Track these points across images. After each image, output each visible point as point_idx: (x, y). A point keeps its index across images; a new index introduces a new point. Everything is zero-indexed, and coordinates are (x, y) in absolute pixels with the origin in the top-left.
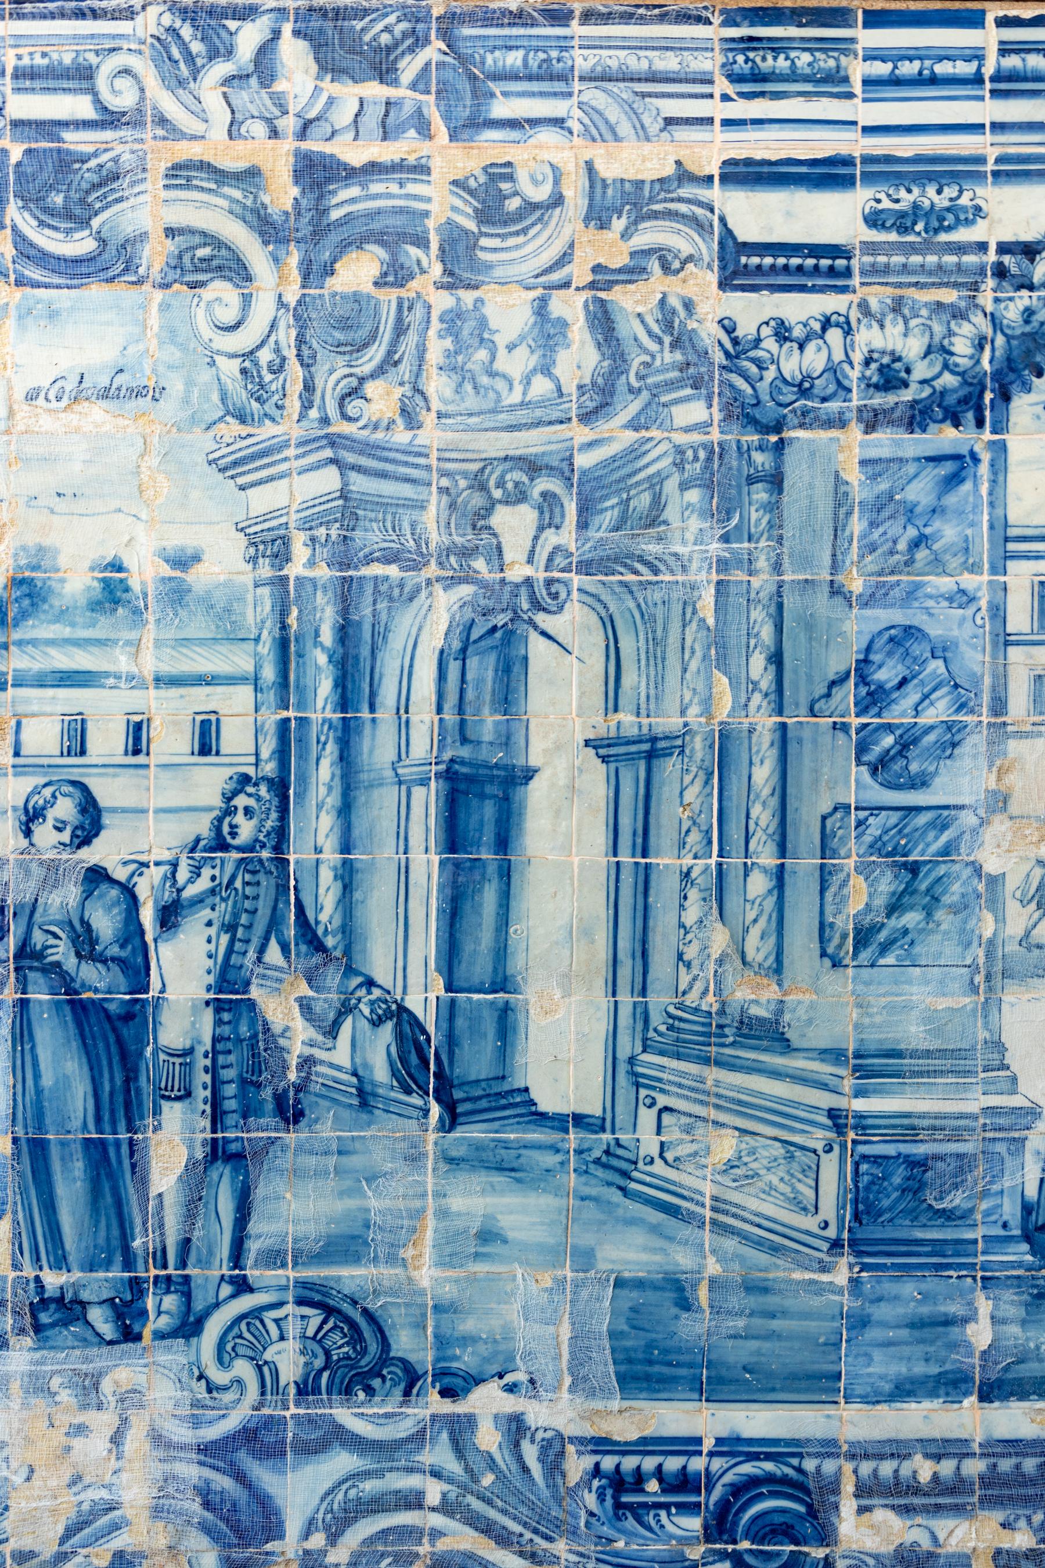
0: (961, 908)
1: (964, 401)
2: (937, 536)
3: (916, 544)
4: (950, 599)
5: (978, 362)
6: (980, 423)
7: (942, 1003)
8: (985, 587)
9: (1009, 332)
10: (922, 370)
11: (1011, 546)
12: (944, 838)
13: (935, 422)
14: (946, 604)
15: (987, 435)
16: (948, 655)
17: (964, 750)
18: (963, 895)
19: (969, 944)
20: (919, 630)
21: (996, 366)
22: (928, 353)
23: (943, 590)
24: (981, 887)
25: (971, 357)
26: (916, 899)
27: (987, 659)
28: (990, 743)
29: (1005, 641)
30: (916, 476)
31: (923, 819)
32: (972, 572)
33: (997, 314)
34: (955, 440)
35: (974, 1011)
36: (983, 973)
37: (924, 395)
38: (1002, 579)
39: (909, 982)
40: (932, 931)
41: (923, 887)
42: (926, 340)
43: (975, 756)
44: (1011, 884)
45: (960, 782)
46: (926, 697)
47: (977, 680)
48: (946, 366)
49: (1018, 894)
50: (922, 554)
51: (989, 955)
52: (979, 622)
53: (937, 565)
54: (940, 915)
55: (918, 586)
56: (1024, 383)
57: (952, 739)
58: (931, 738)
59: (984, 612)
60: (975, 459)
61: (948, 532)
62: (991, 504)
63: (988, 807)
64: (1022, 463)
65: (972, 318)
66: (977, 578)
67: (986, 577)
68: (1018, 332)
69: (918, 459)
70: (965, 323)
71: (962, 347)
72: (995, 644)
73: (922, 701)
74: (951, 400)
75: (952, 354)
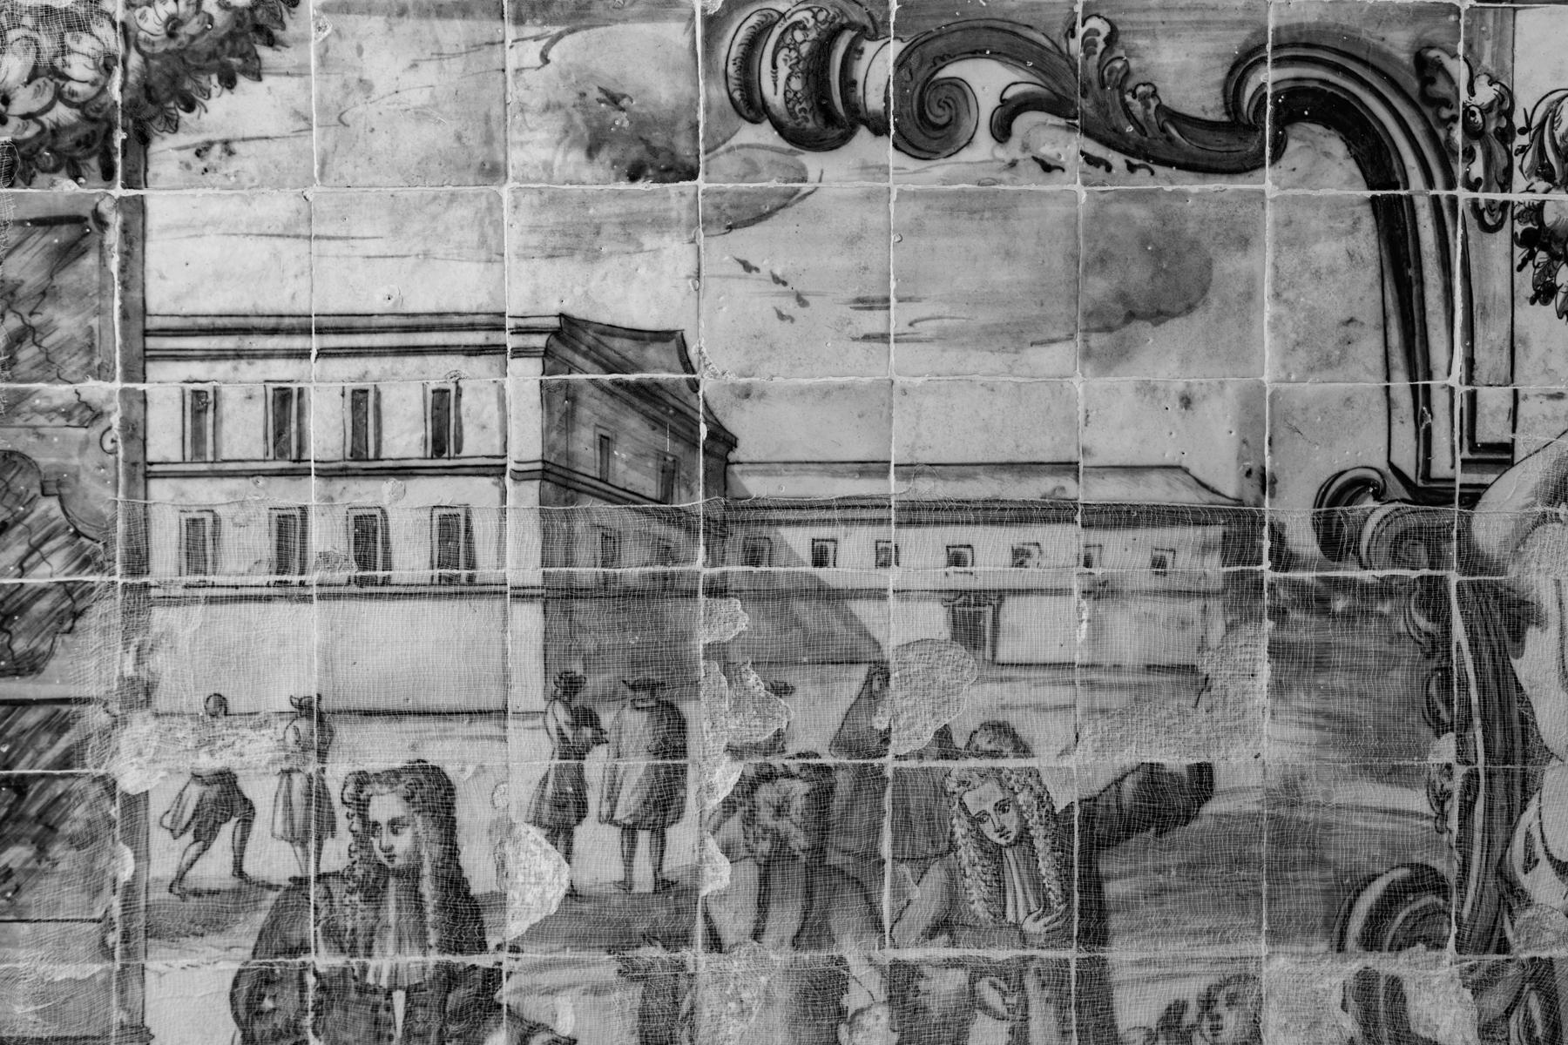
0: (85, 841)
1: (85, 143)
2: (49, 328)
3: (16, 340)
4: (68, 415)
5: (103, 90)
6: (108, 174)
7: (62, 972)
8: (117, 398)
9: (145, 48)
10: (24, 101)
11: (152, 342)
12: (63, 743)
13: (43, 171)
14: (61, 421)
15: (118, 191)
16: (66, 491)
17: (91, 620)
18: (89, 823)
19: (98, 891)
20: (24, 457)
21: (129, 96)
22: (34, 75)
23: (57, 402)
24: (115, 811)
25: (94, 83)
26: (23, 827)
27: (121, 496)
28: (128, 613)
29: (142, 472)
30: (18, 246)
31: (32, 718)
32: (99, 377)
33: (132, 25)
34: (73, 197)
35: (106, 984)
36: (119, 931)
37: (29, 134)
38: (140, 387)
39: (14, 943)
40: (45, 873)
41: (33, 811)
42: (31, 59)
43: (104, 632)
44: (158, 806)
45: (87, 666)
46: (34, 549)
47: (107, 528)
48: (58, 95)
49: (167, 821)
50: (27, 353)
51: (128, 906)
52: (108, 446)
53: (49, 367)
54: (57, 849)
55: (23, 396)
56: (168, 119)
57: (71, 608)
58: (43, 605)
59: (116, 432)
60: (102, 223)
61: (65, 322)
62: (124, 284)
63: (124, 700)
64: (166, 228)
65: (96, 30)
66: (107, 385)
67: (118, 385)
68: (160, 49)
69: (21, 223)
70: (85, 36)
71: (80, 69)
72: (131, 478)
73: (29, 554)
74: (67, 141)
75: (68, 78)
